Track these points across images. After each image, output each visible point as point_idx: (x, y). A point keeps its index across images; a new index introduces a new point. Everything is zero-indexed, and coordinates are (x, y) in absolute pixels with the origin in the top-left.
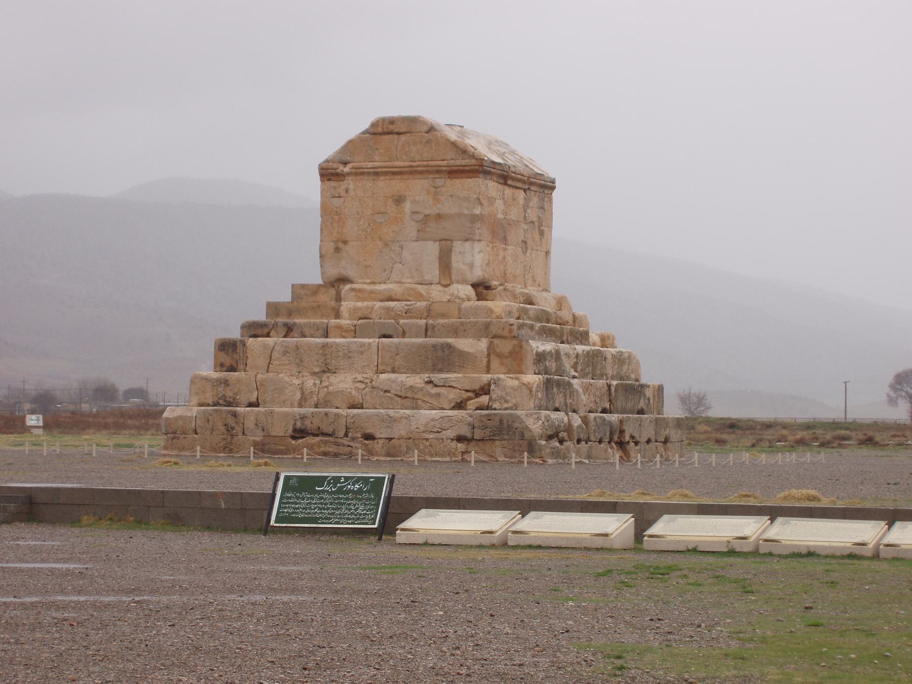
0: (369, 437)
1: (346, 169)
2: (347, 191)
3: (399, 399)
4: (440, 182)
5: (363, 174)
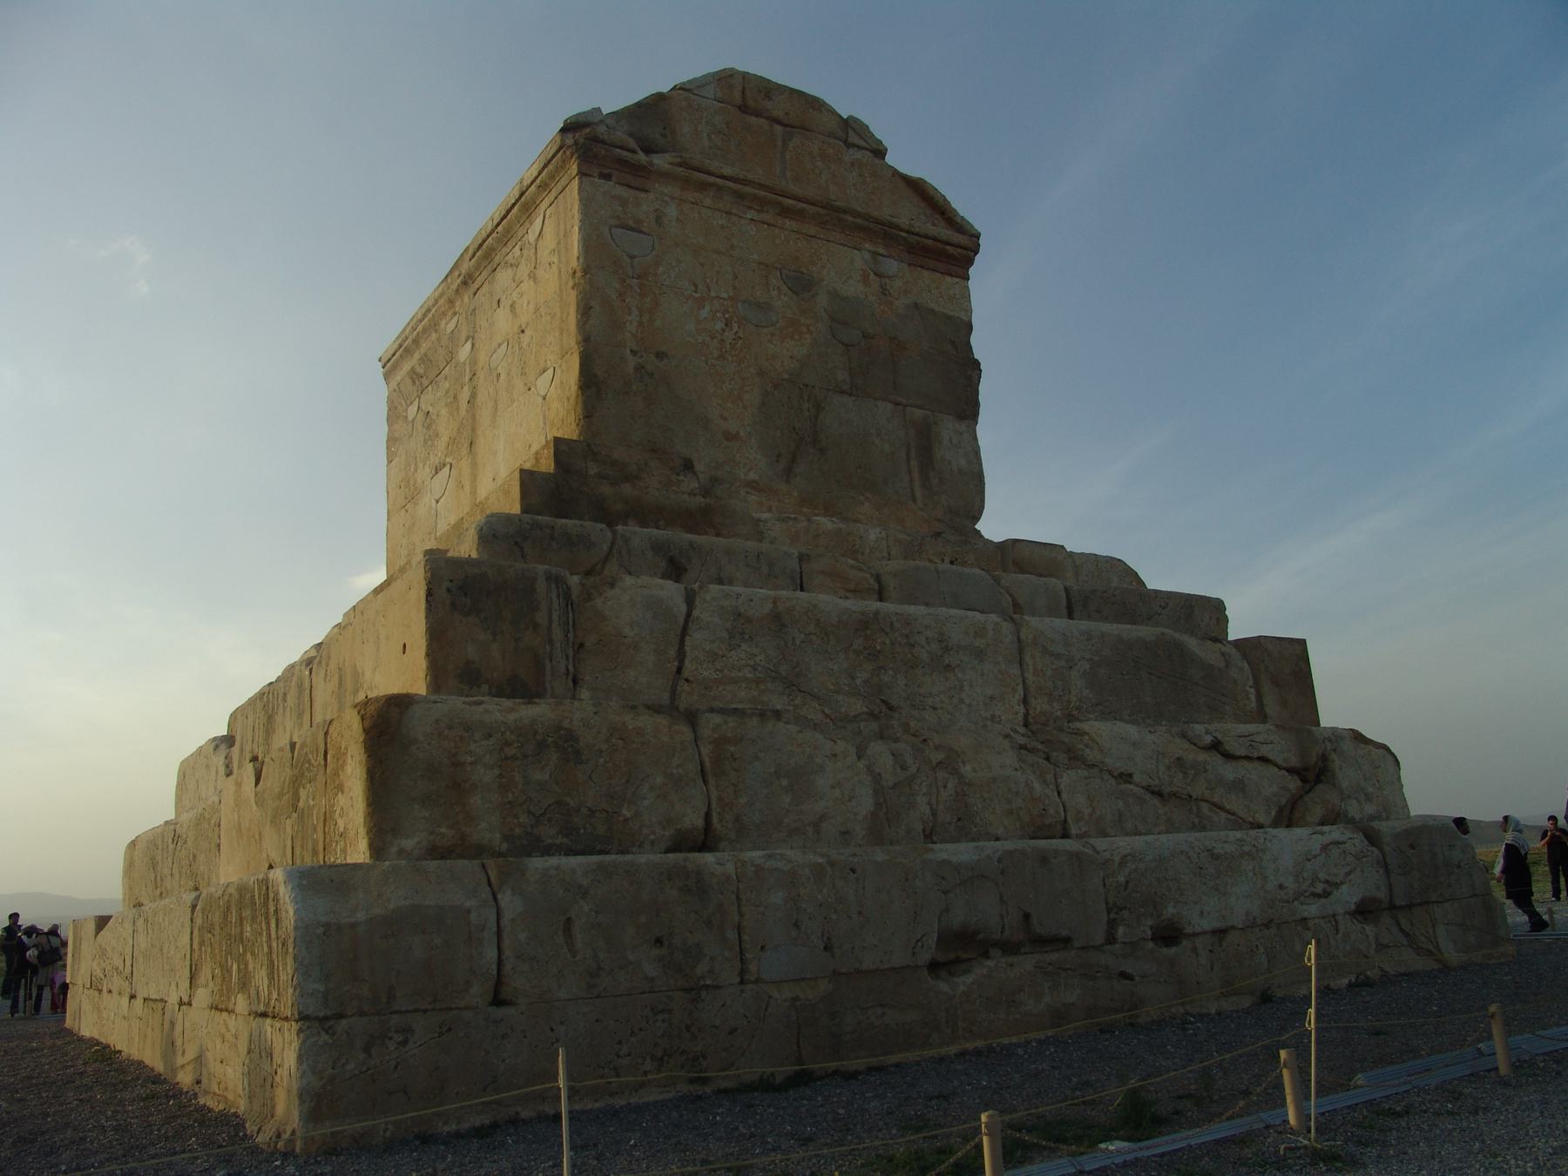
0: (1169, 935)
1: (660, 161)
3: (1156, 801)
4: (891, 266)
5: (703, 187)
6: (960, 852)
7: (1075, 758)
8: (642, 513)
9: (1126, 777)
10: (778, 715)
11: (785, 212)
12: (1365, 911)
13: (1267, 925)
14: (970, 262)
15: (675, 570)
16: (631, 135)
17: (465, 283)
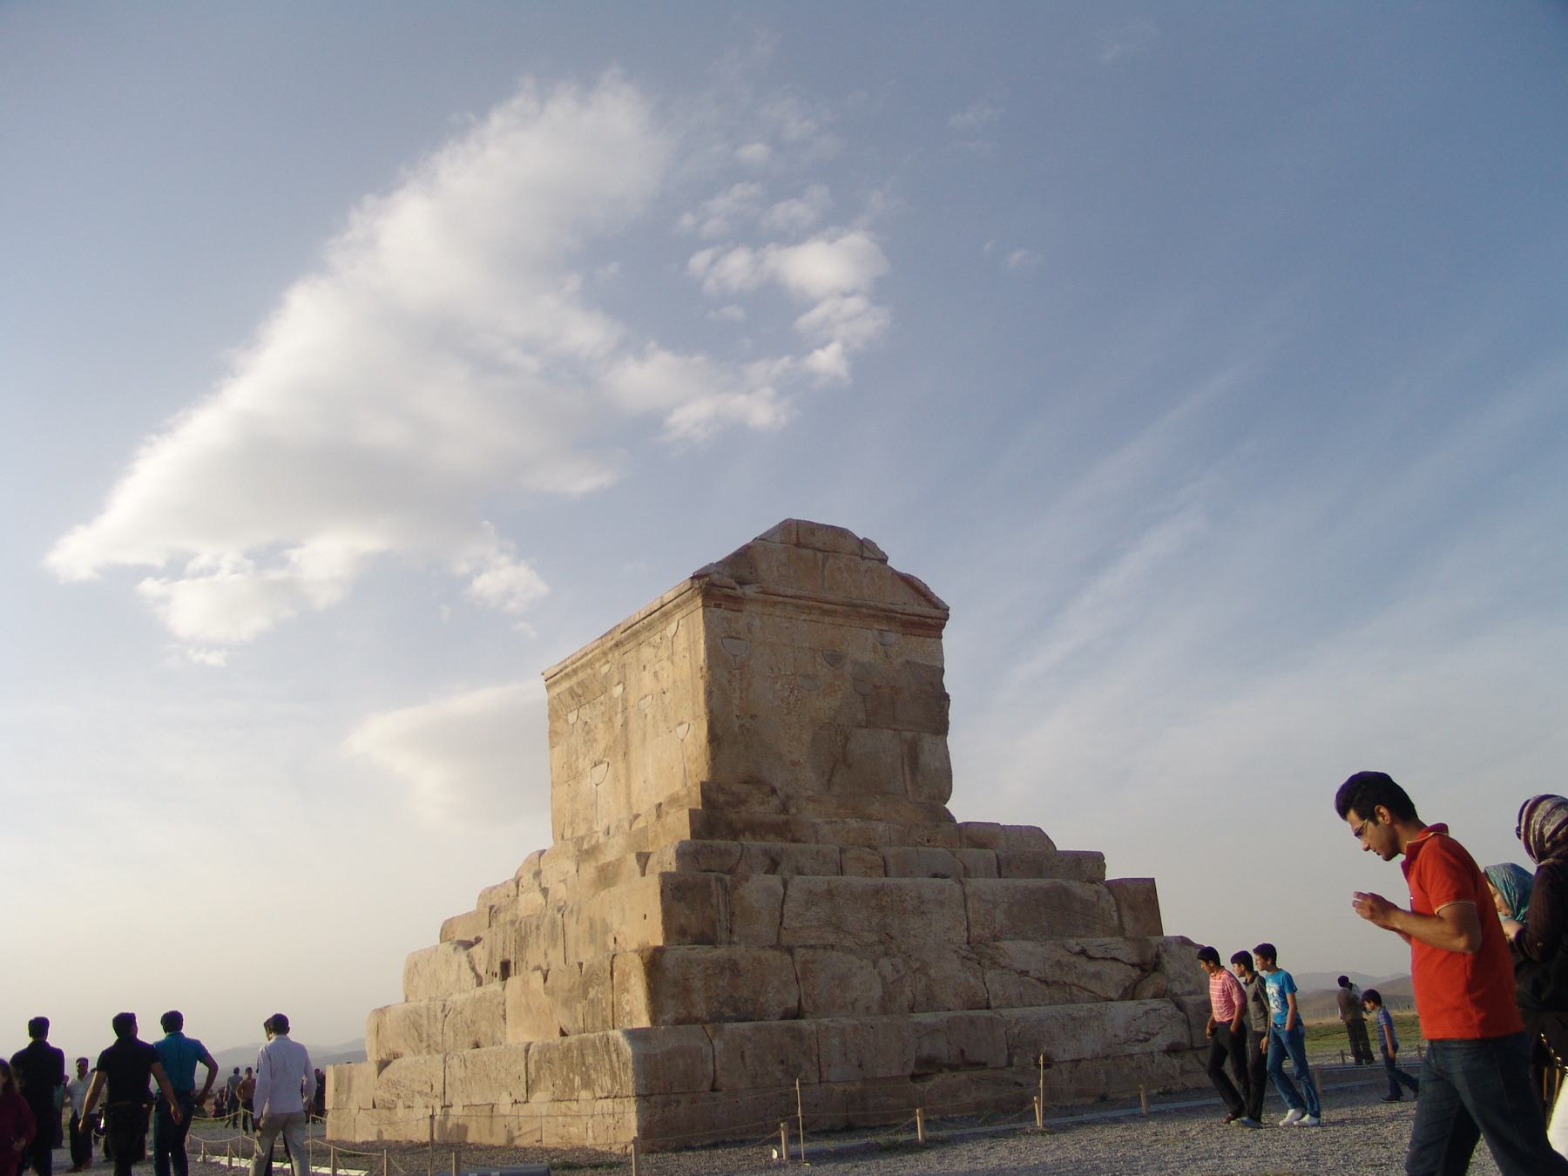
1: (750, 591)
4: (891, 637)
5: (775, 604)
6: (927, 1018)
7: (995, 963)
8: (756, 829)
9: (1025, 973)
10: (832, 947)
11: (825, 612)
12: (1173, 1050)
13: (1107, 1057)
14: (943, 626)
15: (773, 866)
16: (731, 576)
17: (617, 645)
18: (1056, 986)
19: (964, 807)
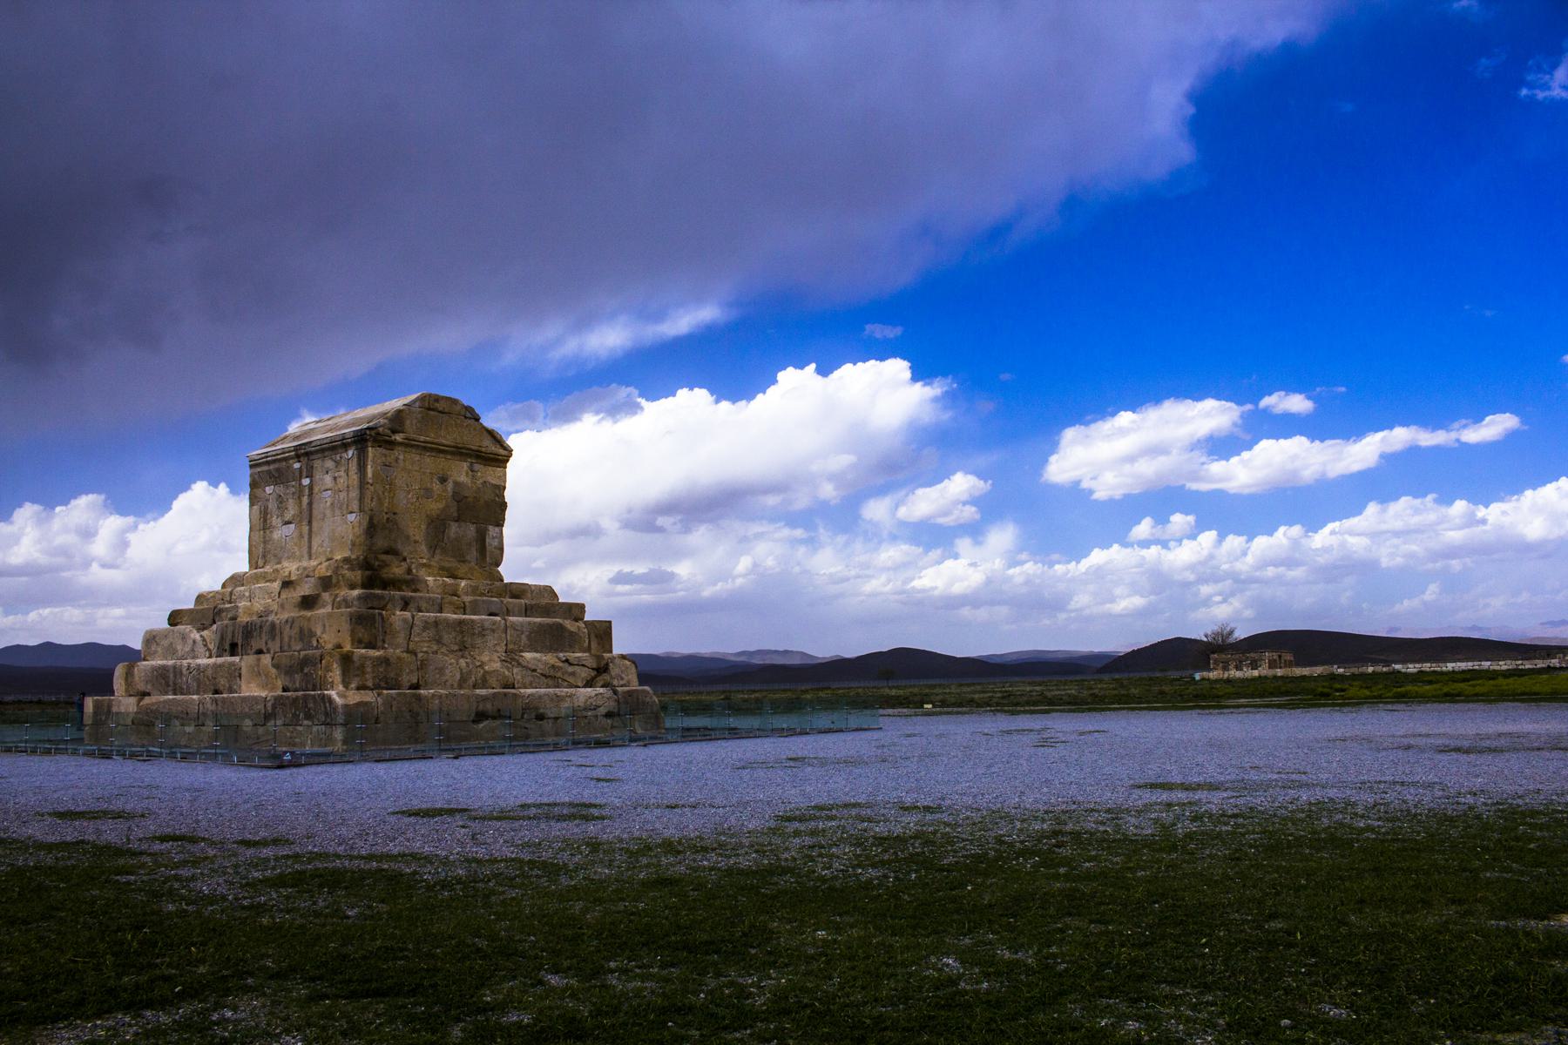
0: (541, 717)
1: (398, 437)
2: (397, 460)
4: (477, 467)
6: (483, 692)
12: (609, 715)
15: (406, 605)
18: (551, 677)
19: (510, 571)
